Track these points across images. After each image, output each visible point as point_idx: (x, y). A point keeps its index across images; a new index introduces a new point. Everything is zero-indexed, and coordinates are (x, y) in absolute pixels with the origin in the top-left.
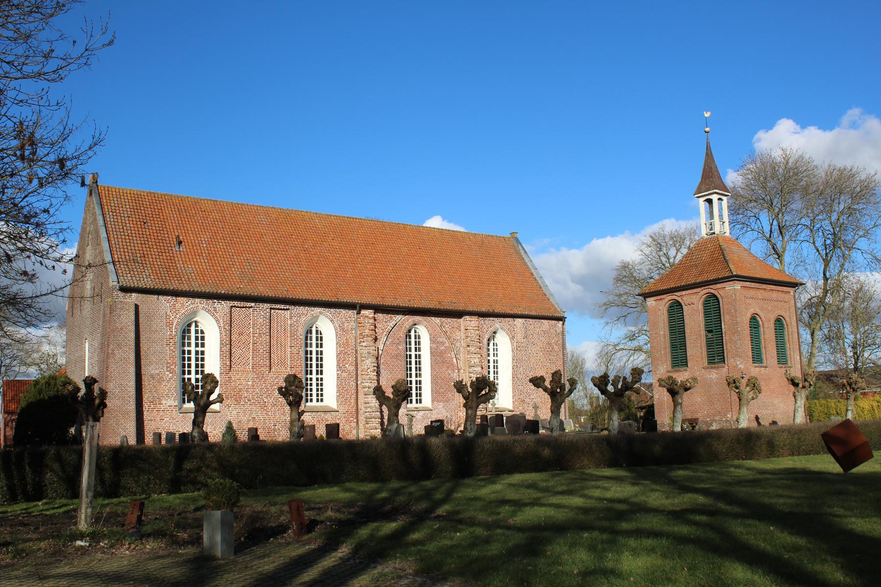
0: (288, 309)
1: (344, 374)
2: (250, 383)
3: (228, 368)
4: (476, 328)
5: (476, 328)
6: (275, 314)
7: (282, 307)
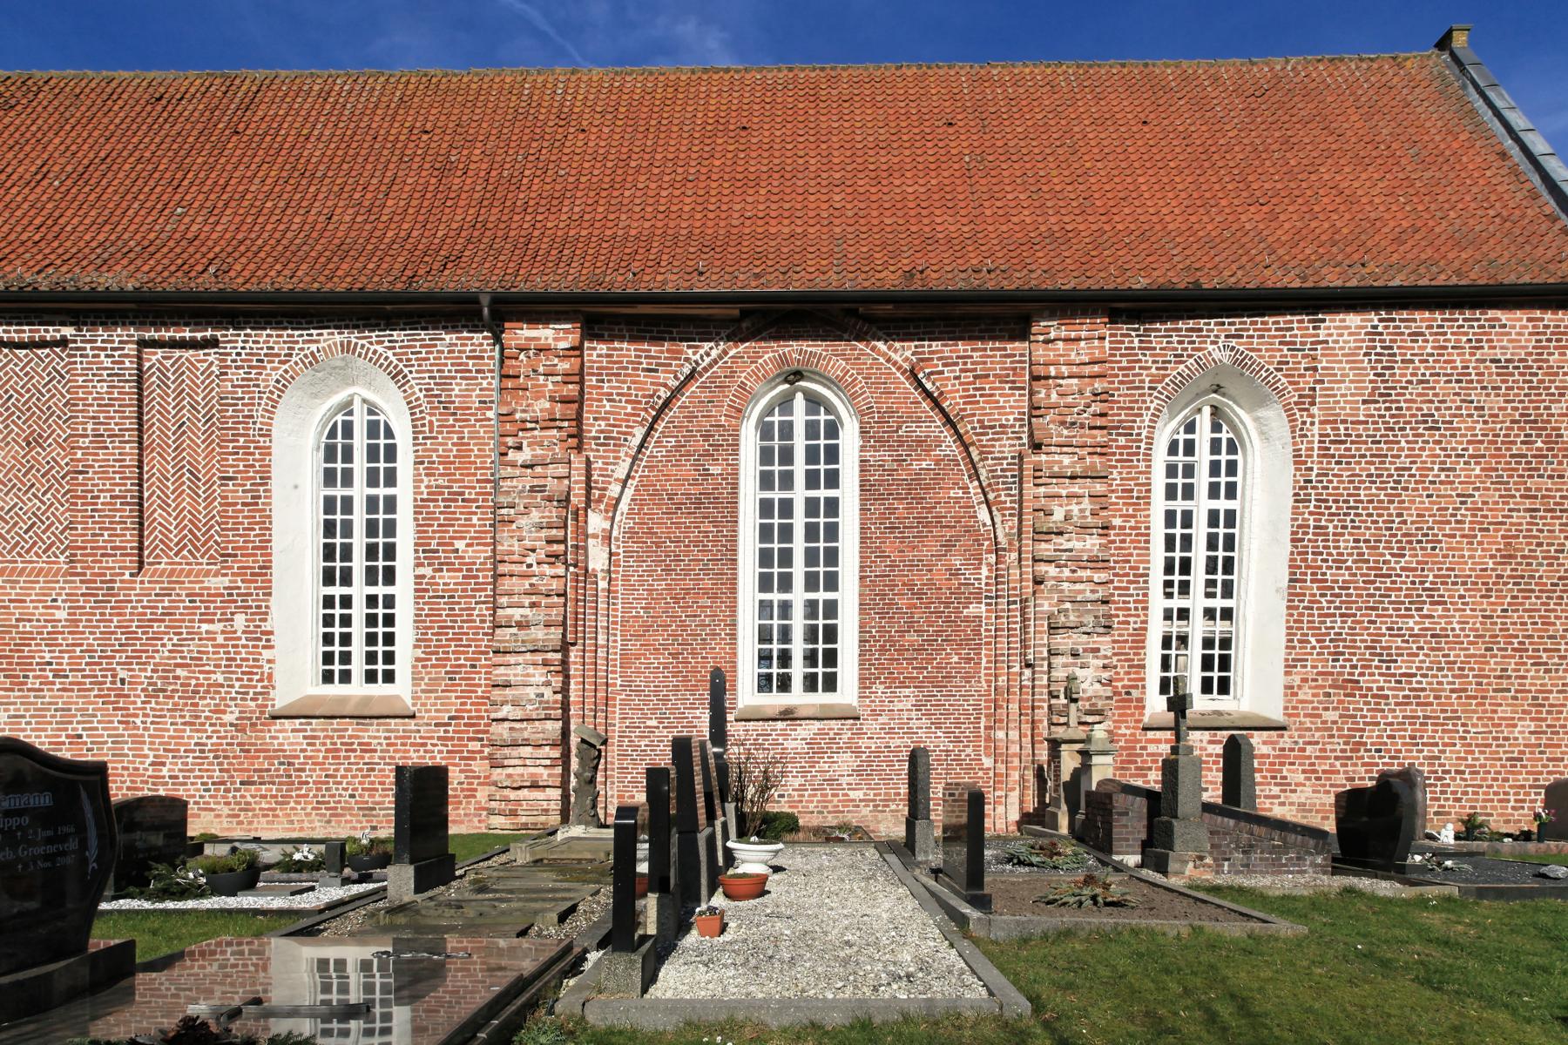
0: (213, 343)
1: (446, 577)
2: (61, 615)
6: (168, 363)
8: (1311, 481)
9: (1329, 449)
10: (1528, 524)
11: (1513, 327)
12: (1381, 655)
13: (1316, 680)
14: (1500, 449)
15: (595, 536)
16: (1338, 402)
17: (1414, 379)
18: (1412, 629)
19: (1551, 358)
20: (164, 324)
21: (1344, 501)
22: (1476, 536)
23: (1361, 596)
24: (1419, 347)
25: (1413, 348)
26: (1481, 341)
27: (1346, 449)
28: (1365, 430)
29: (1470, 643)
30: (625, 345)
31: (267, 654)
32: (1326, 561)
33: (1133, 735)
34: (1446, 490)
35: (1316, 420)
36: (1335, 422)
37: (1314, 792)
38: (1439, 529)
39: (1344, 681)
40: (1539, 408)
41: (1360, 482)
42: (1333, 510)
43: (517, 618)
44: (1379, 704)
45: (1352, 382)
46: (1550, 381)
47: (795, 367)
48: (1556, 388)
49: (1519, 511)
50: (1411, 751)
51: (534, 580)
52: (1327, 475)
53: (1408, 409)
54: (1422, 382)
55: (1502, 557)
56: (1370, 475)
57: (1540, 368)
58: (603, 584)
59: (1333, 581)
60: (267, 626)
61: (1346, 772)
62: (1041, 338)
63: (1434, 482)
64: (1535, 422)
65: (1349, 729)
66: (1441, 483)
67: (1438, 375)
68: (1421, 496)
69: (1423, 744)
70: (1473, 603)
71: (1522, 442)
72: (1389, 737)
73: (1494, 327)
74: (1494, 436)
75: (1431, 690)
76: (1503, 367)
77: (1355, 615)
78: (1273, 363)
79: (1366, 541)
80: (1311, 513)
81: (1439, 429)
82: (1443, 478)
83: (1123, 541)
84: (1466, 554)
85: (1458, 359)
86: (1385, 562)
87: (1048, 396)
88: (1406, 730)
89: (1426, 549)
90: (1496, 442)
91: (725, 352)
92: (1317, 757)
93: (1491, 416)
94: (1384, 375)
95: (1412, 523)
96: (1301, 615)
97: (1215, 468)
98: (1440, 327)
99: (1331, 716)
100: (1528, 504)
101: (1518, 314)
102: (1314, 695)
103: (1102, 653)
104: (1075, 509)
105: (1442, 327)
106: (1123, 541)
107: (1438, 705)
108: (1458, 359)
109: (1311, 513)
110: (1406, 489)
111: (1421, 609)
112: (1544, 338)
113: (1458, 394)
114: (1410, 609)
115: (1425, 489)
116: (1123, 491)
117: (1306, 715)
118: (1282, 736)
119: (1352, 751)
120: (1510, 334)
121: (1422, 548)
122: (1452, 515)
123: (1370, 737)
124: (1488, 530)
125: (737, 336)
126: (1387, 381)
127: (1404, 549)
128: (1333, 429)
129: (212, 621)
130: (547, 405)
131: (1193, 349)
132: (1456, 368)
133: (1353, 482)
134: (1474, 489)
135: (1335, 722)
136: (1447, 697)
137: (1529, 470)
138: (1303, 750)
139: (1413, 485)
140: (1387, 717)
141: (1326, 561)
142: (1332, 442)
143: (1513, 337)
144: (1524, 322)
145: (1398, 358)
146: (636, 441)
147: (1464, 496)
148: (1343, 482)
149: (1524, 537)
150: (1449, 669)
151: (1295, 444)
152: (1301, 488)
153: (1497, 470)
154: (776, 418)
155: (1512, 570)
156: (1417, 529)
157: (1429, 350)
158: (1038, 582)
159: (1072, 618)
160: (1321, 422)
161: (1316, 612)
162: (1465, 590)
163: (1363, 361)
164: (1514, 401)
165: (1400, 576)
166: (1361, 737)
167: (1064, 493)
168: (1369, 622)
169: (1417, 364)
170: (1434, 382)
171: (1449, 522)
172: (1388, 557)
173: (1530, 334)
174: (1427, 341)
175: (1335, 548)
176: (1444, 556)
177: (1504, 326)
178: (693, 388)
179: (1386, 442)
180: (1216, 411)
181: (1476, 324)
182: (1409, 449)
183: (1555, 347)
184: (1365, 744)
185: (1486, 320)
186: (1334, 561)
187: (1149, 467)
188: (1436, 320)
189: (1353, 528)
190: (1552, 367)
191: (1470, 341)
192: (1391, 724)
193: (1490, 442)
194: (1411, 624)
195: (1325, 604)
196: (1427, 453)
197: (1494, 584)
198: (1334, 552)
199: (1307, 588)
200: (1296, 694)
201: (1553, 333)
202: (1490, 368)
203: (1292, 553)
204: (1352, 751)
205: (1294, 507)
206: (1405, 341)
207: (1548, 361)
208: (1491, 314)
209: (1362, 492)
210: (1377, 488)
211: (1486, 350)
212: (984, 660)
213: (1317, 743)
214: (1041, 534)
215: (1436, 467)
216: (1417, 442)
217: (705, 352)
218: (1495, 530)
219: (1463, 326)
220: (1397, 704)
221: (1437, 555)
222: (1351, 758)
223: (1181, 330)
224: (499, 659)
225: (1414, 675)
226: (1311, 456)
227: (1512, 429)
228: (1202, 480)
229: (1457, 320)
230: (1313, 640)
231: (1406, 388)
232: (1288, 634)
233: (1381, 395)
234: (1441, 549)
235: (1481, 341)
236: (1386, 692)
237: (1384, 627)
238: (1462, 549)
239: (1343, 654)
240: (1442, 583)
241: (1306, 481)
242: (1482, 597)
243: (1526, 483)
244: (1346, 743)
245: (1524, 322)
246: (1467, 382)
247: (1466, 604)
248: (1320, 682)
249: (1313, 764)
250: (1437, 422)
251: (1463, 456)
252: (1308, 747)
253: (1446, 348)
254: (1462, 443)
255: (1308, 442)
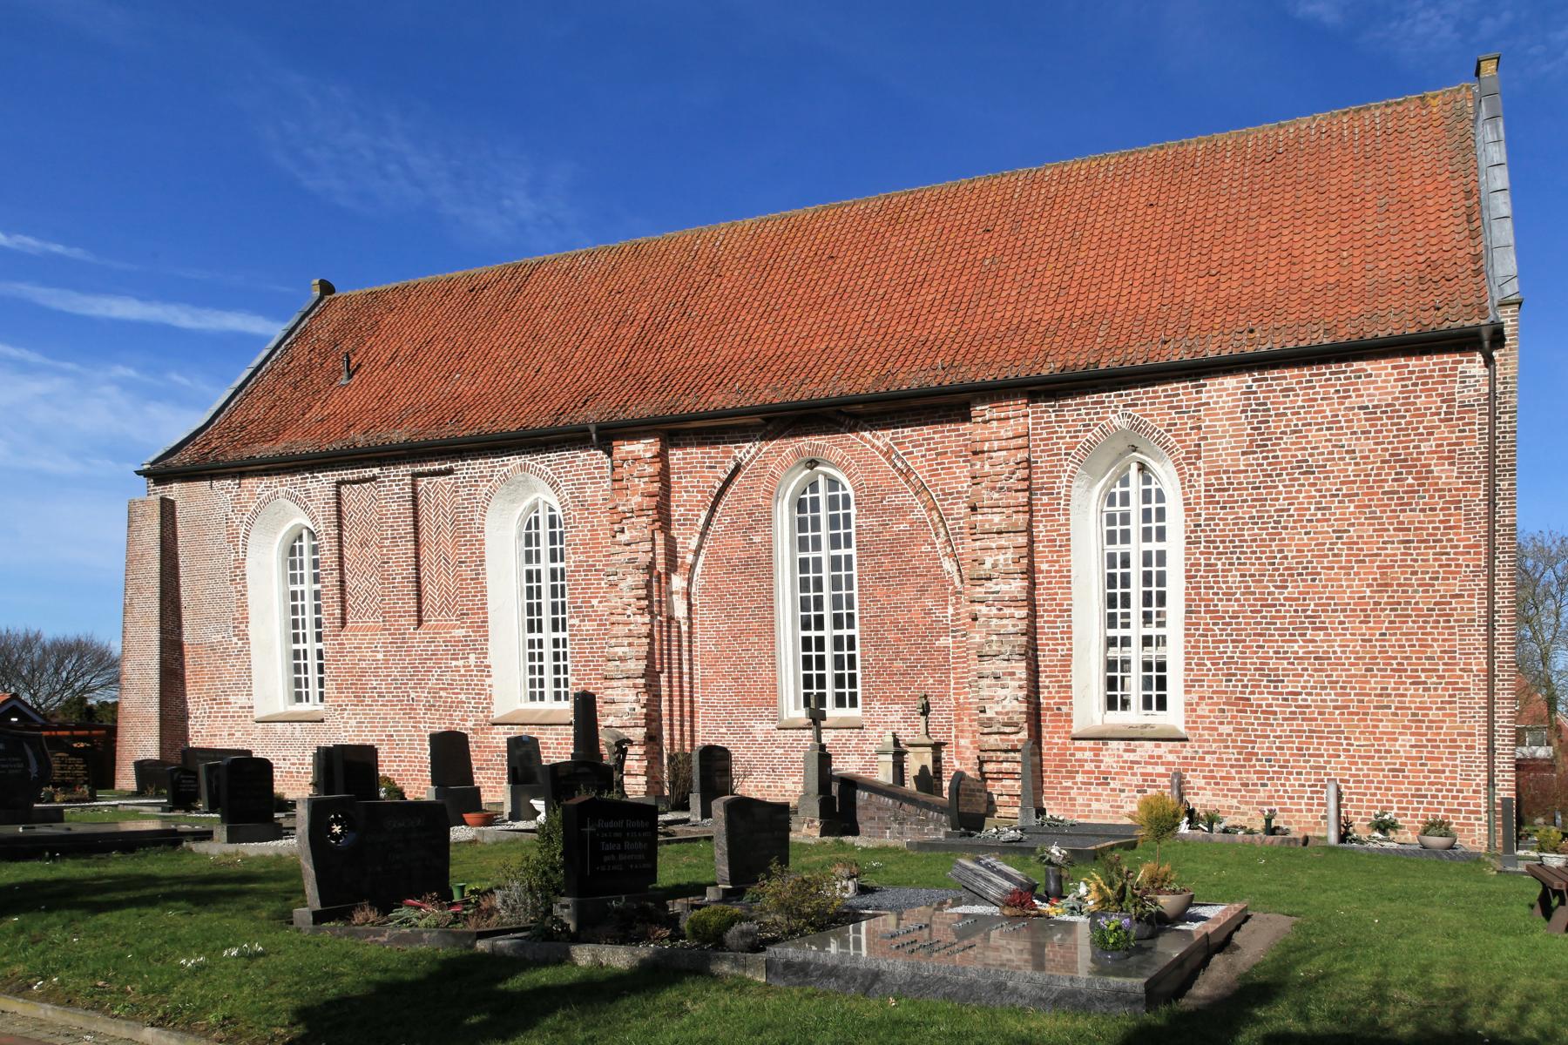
0: (449, 472)
2: (380, 656)
3: (338, 623)
4: (1020, 441)
5: (1020, 441)
6: (430, 486)
7: (436, 466)
8: (1200, 525)
9: (1214, 496)
10: (1402, 554)
11: (1380, 376)
12: (1269, 675)
13: (1212, 698)
14: (1372, 487)
15: (678, 593)
16: (1221, 455)
17: (1288, 430)
18: (1297, 653)
19: (1418, 401)
20: (425, 461)
21: (1230, 542)
22: (1352, 568)
23: (1249, 624)
24: (1291, 402)
25: (1285, 403)
26: (1348, 391)
27: (1229, 496)
28: (1245, 478)
29: (1352, 664)
30: (694, 450)
31: (488, 681)
32: (1217, 594)
33: (1064, 744)
34: (1322, 527)
35: (1202, 472)
36: (1218, 472)
37: (1214, 795)
38: (1318, 562)
39: (1237, 698)
40: (1408, 448)
41: (1243, 524)
42: (1221, 550)
43: (620, 654)
44: (1268, 719)
45: (1231, 436)
46: (1418, 422)
47: (808, 457)
48: (1424, 428)
49: (1393, 543)
50: (1299, 761)
51: (632, 627)
52: (1214, 519)
53: (1284, 457)
54: (1295, 432)
55: (1378, 585)
56: (1253, 518)
57: (1407, 411)
58: (684, 628)
59: (1224, 612)
60: (487, 662)
61: (1240, 779)
62: (980, 419)
63: (1311, 521)
64: (1405, 460)
65: (1242, 741)
66: (1318, 521)
67: (1310, 424)
68: (1299, 533)
69: (1310, 755)
70: (1353, 628)
71: (1394, 480)
72: (1278, 748)
73: (1360, 377)
74: (1366, 475)
75: (1316, 707)
76: (1371, 413)
77: (1244, 641)
78: (1162, 425)
79: (1252, 576)
80: (1201, 553)
81: (1313, 473)
82: (1319, 516)
83: (1050, 583)
84: (1344, 583)
85: (1328, 409)
86: (1269, 594)
87: (983, 467)
88: (1293, 742)
89: (1306, 580)
90: (1368, 482)
91: (760, 450)
92: (1215, 765)
93: (1362, 458)
94: (1260, 428)
95: (1293, 558)
96: (1199, 641)
97: (1146, 515)
98: (1308, 381)
99: (1226, 729)
100: (1401, 536)
101: (1383, 363)
102: (1210, 711)
103: (1018, 676)
104: (1001, 558)
105: (1311, 381)
106: (1050, 583)
107: (1322, 720)
108: (1328, 409)
109: (1201, 553)
110: (1285, 528)
111: (1305, 635)
112: (1410, 383)
113: (1330, 441)
114: (1294, 635)
115: (1302, 527)
116: (1048, 541)
117: (1204, 729)
118: (1185, 746)
119: (1245, 760)
120: (1376, 382)
121: (1303, 580)
122: (1329, 550)
123: (1261, 748)
124: (1364, 561)
125: (768, 436)
126: (1263, 434)
127: (1286, 581)
128: (1216, 479)
129: (457, 659)
130: (640, 499)
131: (1098, 419)
132: (1327, 417)
133: (1237, 524)
134: (1349, 525)
135: (1230, 735)
136: (1331, 714)
137: (1401, 505)
138: (1203, 759)
139: (1291, 524)
140: (1275, 731)
141: (1217, 594)
142: (1216, 490)
143: (1380, 384)
144: (1390, 370)
145: (1272, 413)
146: (702, 521)
147: (1339, 531)
148: (1228, 525)
149: (1399, 567)
150: (1332, 688)
151: (1184, 494)
152: (1192, 532)
153: (1370, 506)
154: (808, 496)
155: (1389, 597)
156: (1297, 563)
157: (1300, 403)
158: (975, 619)
159: (994, 648)
160: (1206, 474)
161: (1210, 639)
162: (1345, 617)
163: (1240, 418)
164: (1383, 443)
165: (1284, 605)
166: (1253, 748)
167: (994, 545)
168: (1258, 647)
169: (1290, 416)
170: (1307, 431)
171: (1327, 556)
172: (1272, 589)
173: (1396, 380)
174: (1298, 395)
175: (1224, 582)
176: (1323, 587)
177: (1370, 375)
178: (739, 479)
179: (1265, 488)
180: (1142, 467)
181: (1342, 376)
182: (1286, 492)
183: (1421, 391)
184: (1257, 754)
185: (1352, 372)
186: (1224, 594)
187: (1068, 520)
188: (1305, 376)
189: (1239, 564)
190: (1419, 409)
191: (1338, 391)
192: (1280, 737)
193: (1362, 482)
194: (1296, 649)
195: (1218, 632)
196: (1303, 494)
197: (1372, 610)
198: (1224, 586)
199: (1201, 618)
200: (1195, 710)
201: (1418, 378)
202: (1359, 414)
203: (1187, 588)
204: (1245, 760)
205: (1186, 549)
206: (1278, 397)
207: (1415, 403)
208: (1356, 365)
209: (1246, 533)
210: (1259, 529)
211: (1354, 399)
212: (952, 682)
213: (1215, 753)
214: (979, 580)
215: (1313, 507)
216: (1293, 486)
217: (746, 451)
218: (1371, 562)
219: (1330, 379)
220: (1284, 719)
221: (1317, 586)
222: (1244, 766)
223: (1087, 403)
224: (607, 684)
225: (1300, 694)
226: (1199, 504)
227: (1383, 468)
228: (1136, 526)
229: (1324, 374)
230: (1208, 663)
231: (1281, 438)
232: (1187, 658)
233: (1258, 446)
234: (1321, 580)
235: (1348, 391)
236: (1274, 709)
237: (1271, 651)
238: (1341, 580)
239: (1235, 675)
240: (1323, 611)
241: (1196, 526)
242: (1361, 622)
243: (1398, 517)
244: (1239, 753)
245: (1390, 370)
246: (1337, 429)
247: (1347, 629)
248: (1215, 700)
249: (1212, 771)
250: (1311, 466)
251: (1338, 495)
252: (1207, 756)
253: (1316, 400)
254: (1335, 484)
255: (1196, 492)
